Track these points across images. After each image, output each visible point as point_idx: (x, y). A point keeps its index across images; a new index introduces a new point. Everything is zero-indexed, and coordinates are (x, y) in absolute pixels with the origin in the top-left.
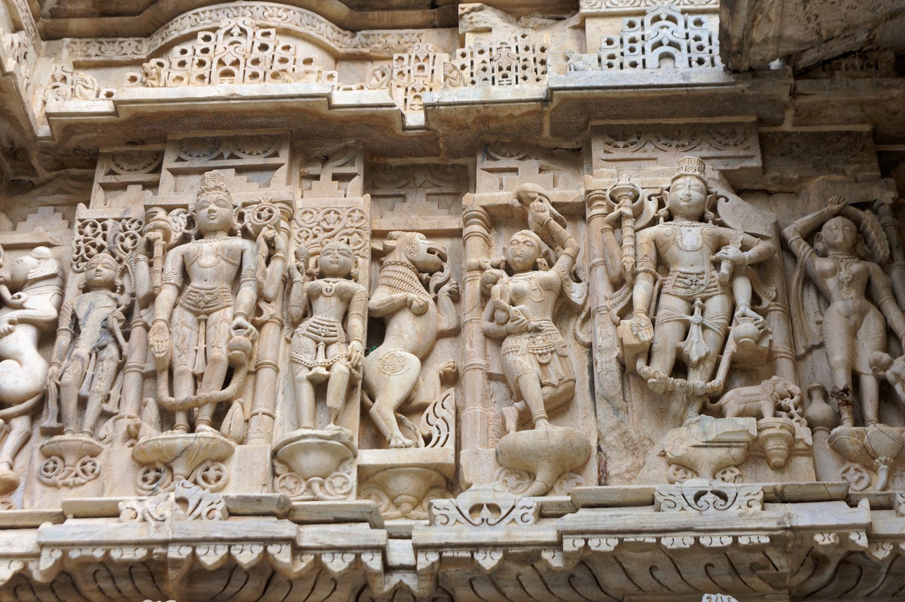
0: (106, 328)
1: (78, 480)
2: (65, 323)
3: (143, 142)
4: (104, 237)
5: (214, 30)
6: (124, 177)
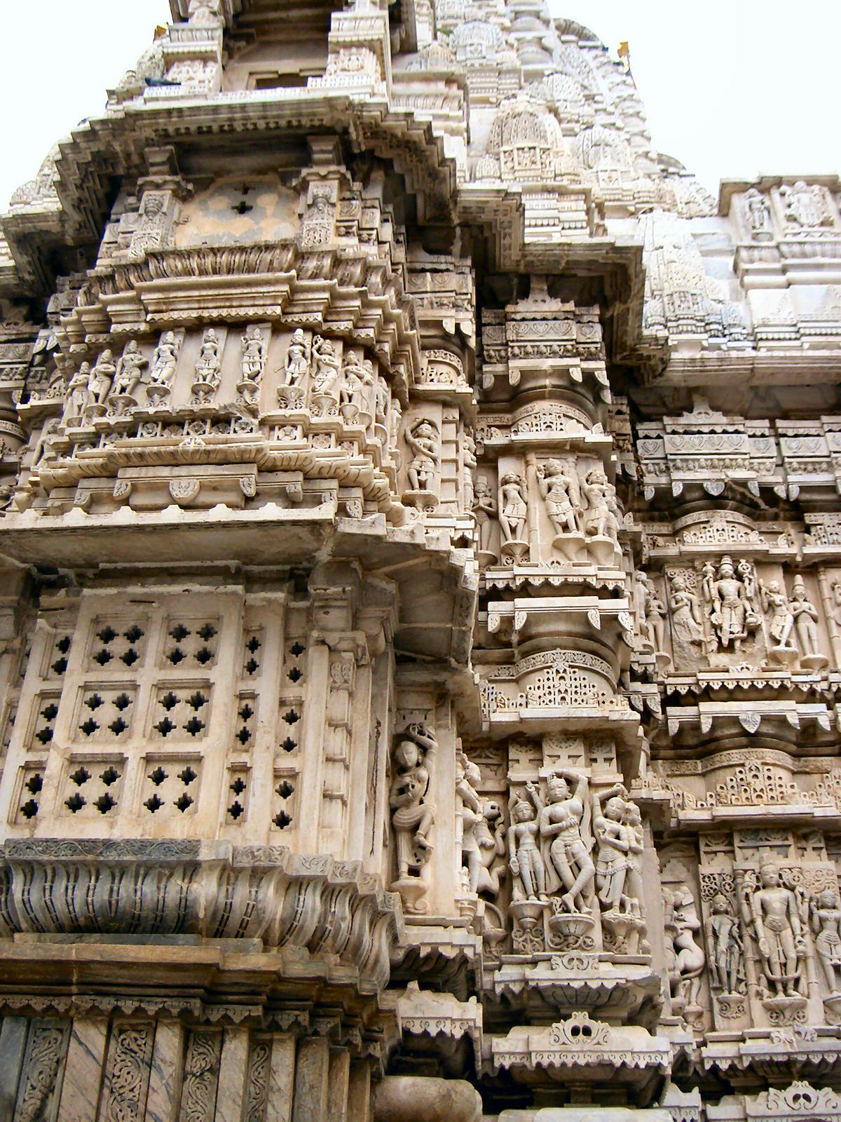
0: (731, 935)
2: (710, 933)
5: (743, 765)
6: (715, 848)
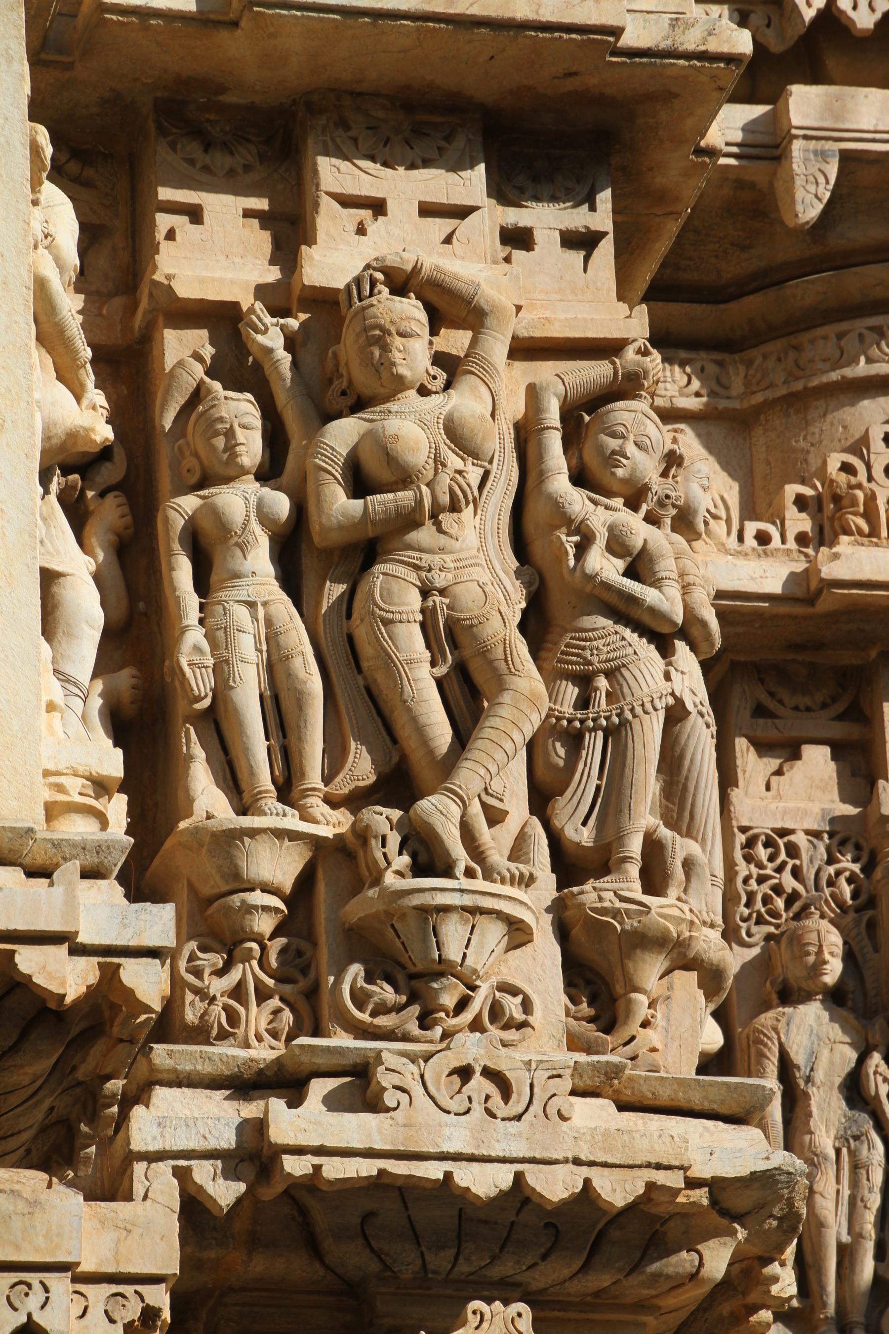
4: (796, 873)
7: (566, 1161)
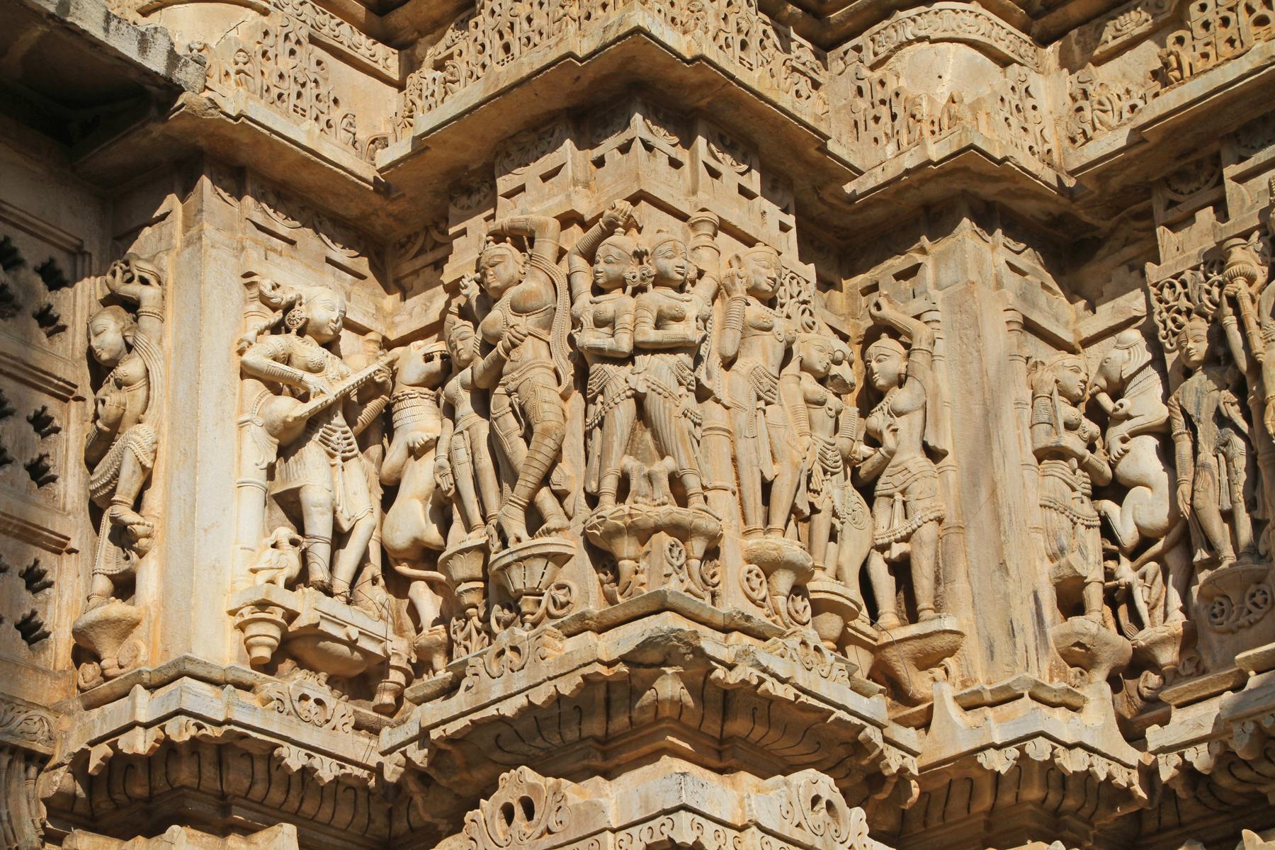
0: (1222, 420)
1: (1252, 618)
2: (1179, 425)
3: (1195, 150)
7: (545, 681)
